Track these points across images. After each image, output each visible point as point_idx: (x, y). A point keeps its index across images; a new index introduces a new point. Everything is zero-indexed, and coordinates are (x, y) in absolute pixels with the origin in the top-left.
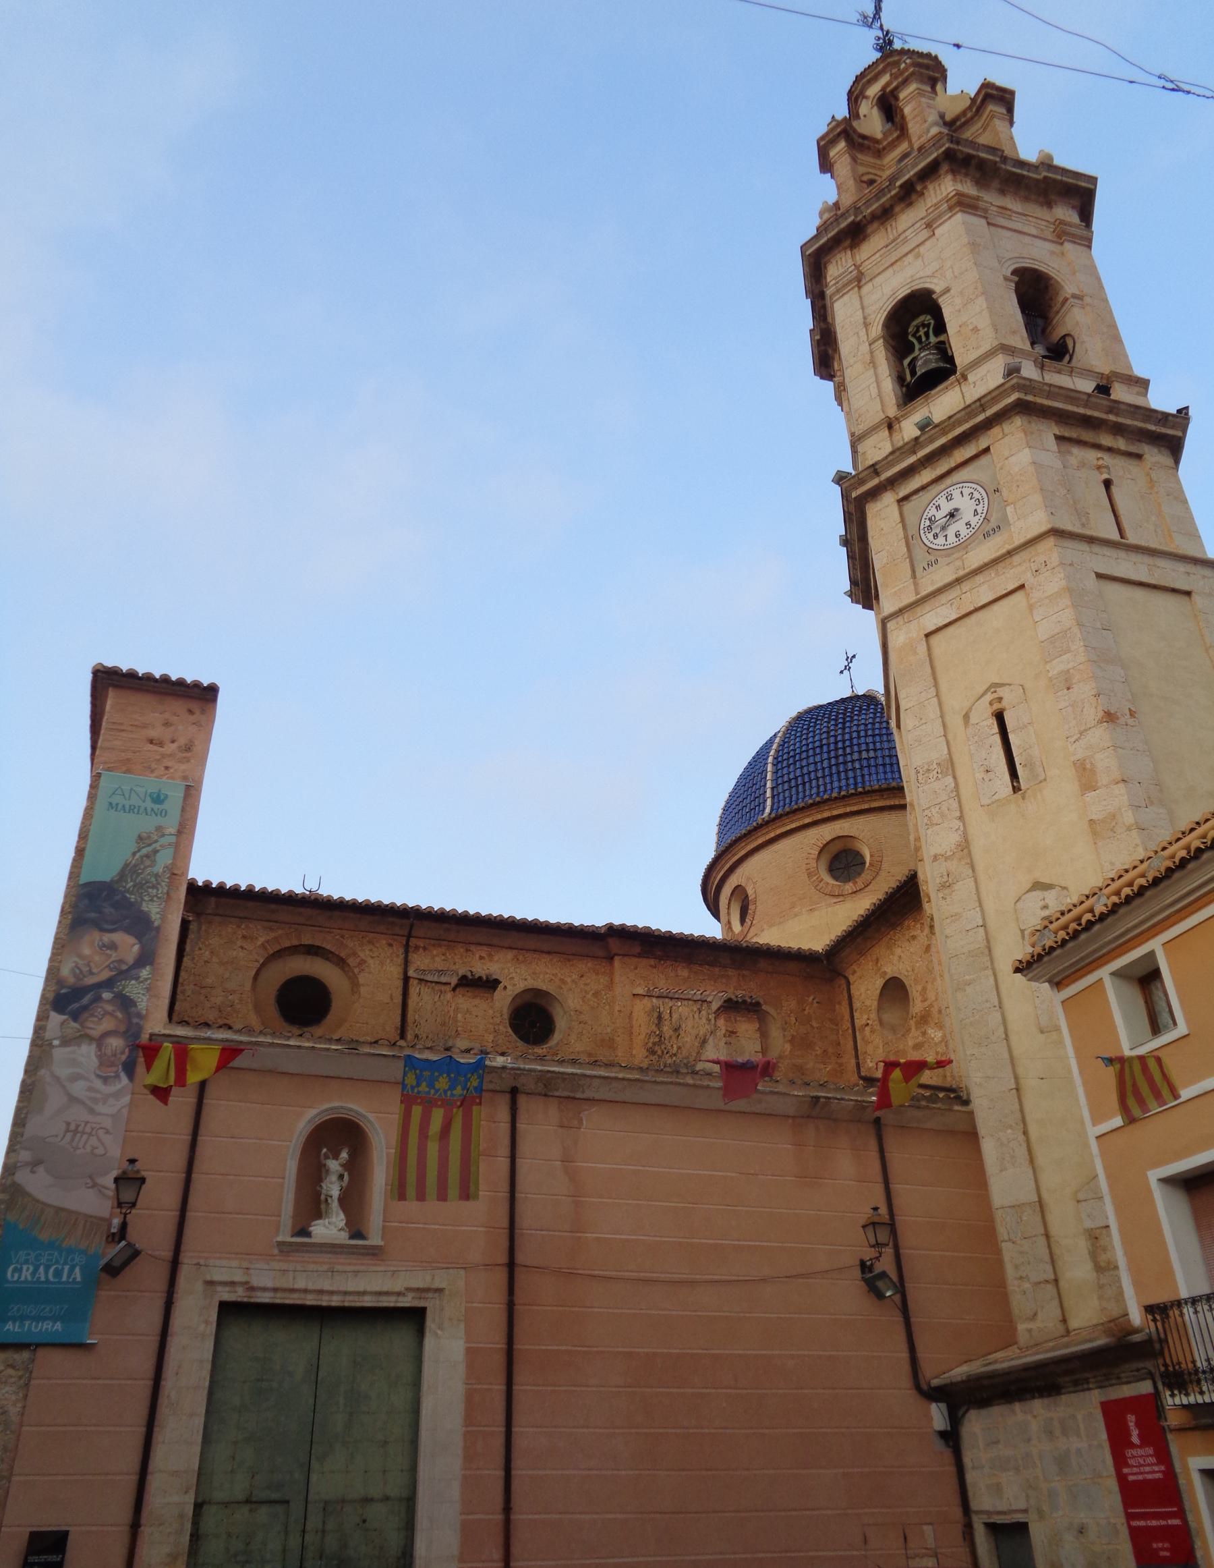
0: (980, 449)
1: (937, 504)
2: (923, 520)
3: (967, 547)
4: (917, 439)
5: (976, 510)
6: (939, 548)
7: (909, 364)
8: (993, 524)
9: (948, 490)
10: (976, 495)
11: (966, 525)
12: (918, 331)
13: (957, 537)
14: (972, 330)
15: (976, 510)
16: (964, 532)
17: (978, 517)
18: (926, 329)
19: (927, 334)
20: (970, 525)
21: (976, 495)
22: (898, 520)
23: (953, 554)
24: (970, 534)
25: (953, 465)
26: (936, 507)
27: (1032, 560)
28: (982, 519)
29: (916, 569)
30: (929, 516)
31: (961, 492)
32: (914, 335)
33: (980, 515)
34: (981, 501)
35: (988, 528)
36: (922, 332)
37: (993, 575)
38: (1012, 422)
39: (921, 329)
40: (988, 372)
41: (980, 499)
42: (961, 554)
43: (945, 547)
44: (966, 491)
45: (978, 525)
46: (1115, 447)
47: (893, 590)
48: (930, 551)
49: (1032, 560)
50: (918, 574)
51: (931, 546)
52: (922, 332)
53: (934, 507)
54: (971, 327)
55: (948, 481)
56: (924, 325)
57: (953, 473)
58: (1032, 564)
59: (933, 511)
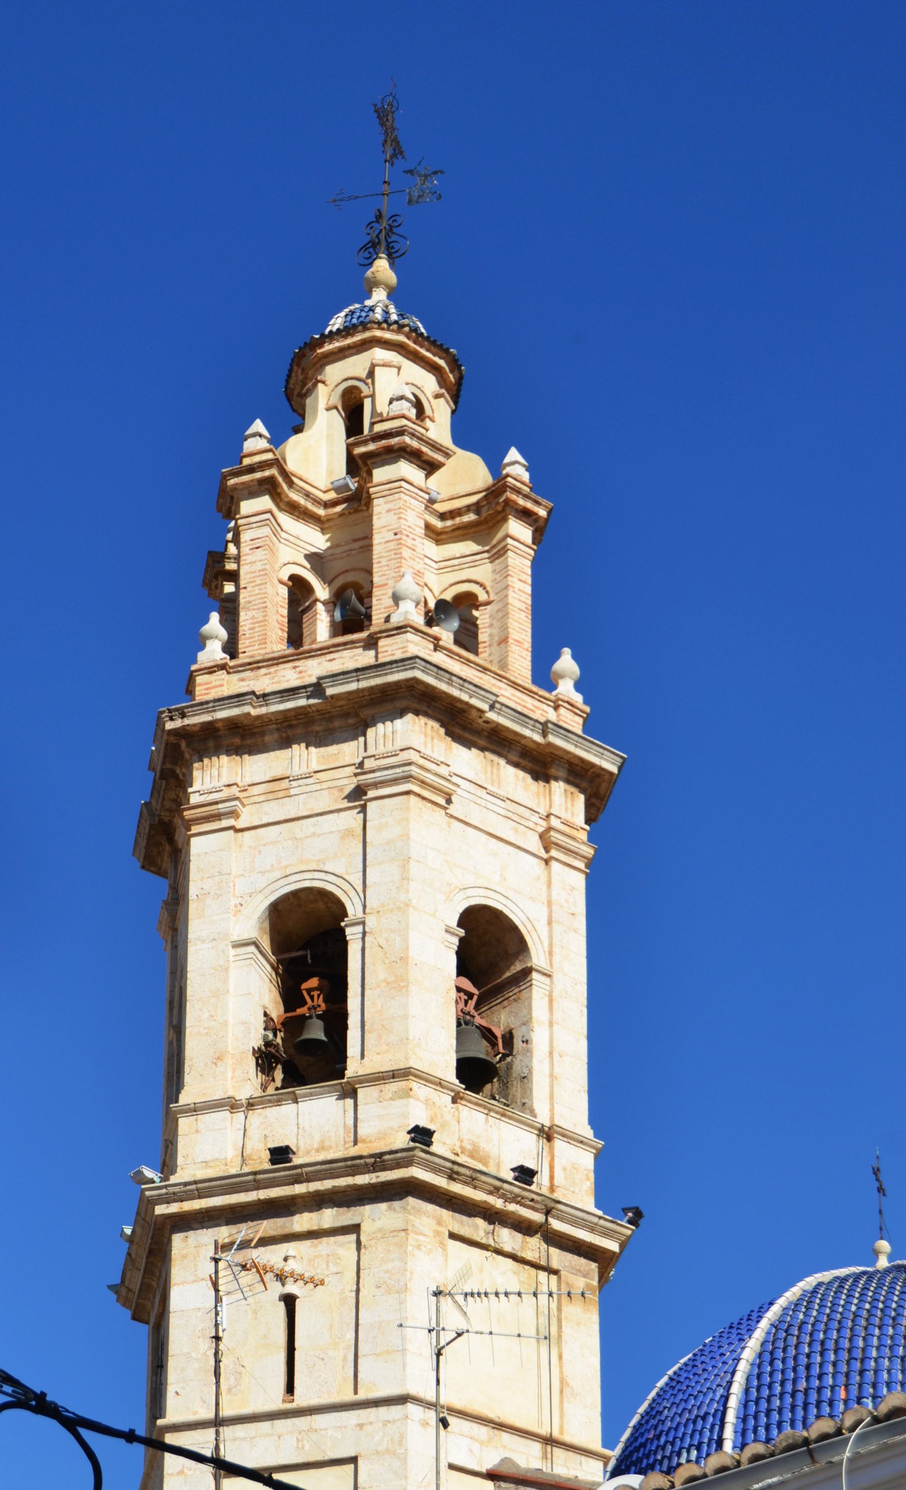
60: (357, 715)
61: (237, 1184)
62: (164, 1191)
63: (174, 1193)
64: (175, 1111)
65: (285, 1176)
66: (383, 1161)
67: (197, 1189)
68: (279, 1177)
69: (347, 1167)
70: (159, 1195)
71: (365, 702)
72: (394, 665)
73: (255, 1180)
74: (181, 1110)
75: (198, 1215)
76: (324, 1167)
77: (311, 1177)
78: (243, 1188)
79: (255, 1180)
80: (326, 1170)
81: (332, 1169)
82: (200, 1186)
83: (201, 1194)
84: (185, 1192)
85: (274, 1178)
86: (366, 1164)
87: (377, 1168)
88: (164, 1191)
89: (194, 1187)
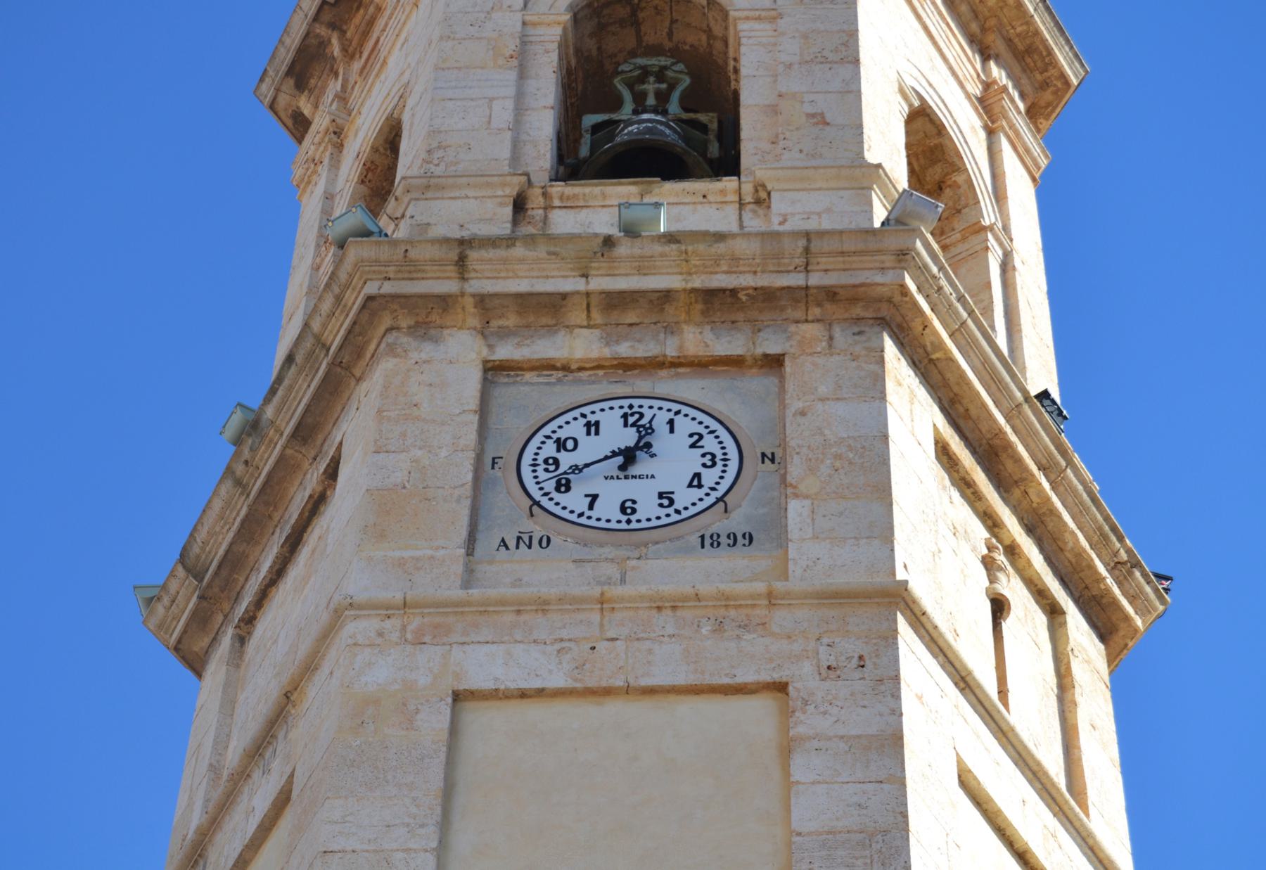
0: (759, 351)
1: (592, 418)
2: (539, 437)
3: (646, 545)
4: (608, 242)
5: (697, 476)
6: (565, 514)
7: (596, 128)
8: (736, 522)
9: (636, 402)
10: (709, 444)
11: (661, 495)
12: (642, 79)
13: (623, 509)
14: (813, 116)
15: (697, 476)
16: (648, 508)
17: (696, 493)
18: (664, 86)
19: (663, 97)
20: (672, 502)
21: (709, 444)
22: (473, 403)
23: (601, 546)
24: (665, 521)
25: (671, 351)
26: (588, 425)
27: (825, 640)
28: (709, 501)
29: (480, 537)
30: (562, 434)
31: (671, 422)
32: (630, 86)
33: (705, 490)
34: (720, 464)
35: (718, 524)
36: (651, 87)
37: (705, 631)
38: (860, 333)
39: (652, 79)
40: (828, 210)
41: (719, 456)
42: (622, 553)
43: (583, 520)
44: (685, 426)
45: (693, 510)
46: (1026, 551)
47: (398, 554)
48: (535, 508)
49: (825, 640)
50: (479, 551)
51: (545, 502)
52: (651, 87)
53: (584, 421)
54: (809, 109)
55: (643, 385)
56: (660, 76)
57: (663, 373)
58: (823, 649)
59: (577, 429)
60: (984, 30)
61: (1001, 381)
62: (935, 269)
63: (940, 289)
64: (879, 177)
65: (1046, 448)
66: (1130, 573)
67: (964, 323)
68: (1040, 439)
69: (1100, 528)
70: (926, 266)
71: (1005, 33)
72: (1067, 48)
73: (1019, 406)
74: (886, 185)
75: (921, 351)
76: (1085, 496)
77: (1062, 489)
78: (998, 394)
79: (1019, 406)
80: (1082, 503)
81: (1087, 509)
82: (970, 322)
83: (957, 334)
84: (951, 305)
85: (1036, 433)
86: (1116, 554)
87: (1117, 572)
88: (935, 269)
89: (965, 315)
